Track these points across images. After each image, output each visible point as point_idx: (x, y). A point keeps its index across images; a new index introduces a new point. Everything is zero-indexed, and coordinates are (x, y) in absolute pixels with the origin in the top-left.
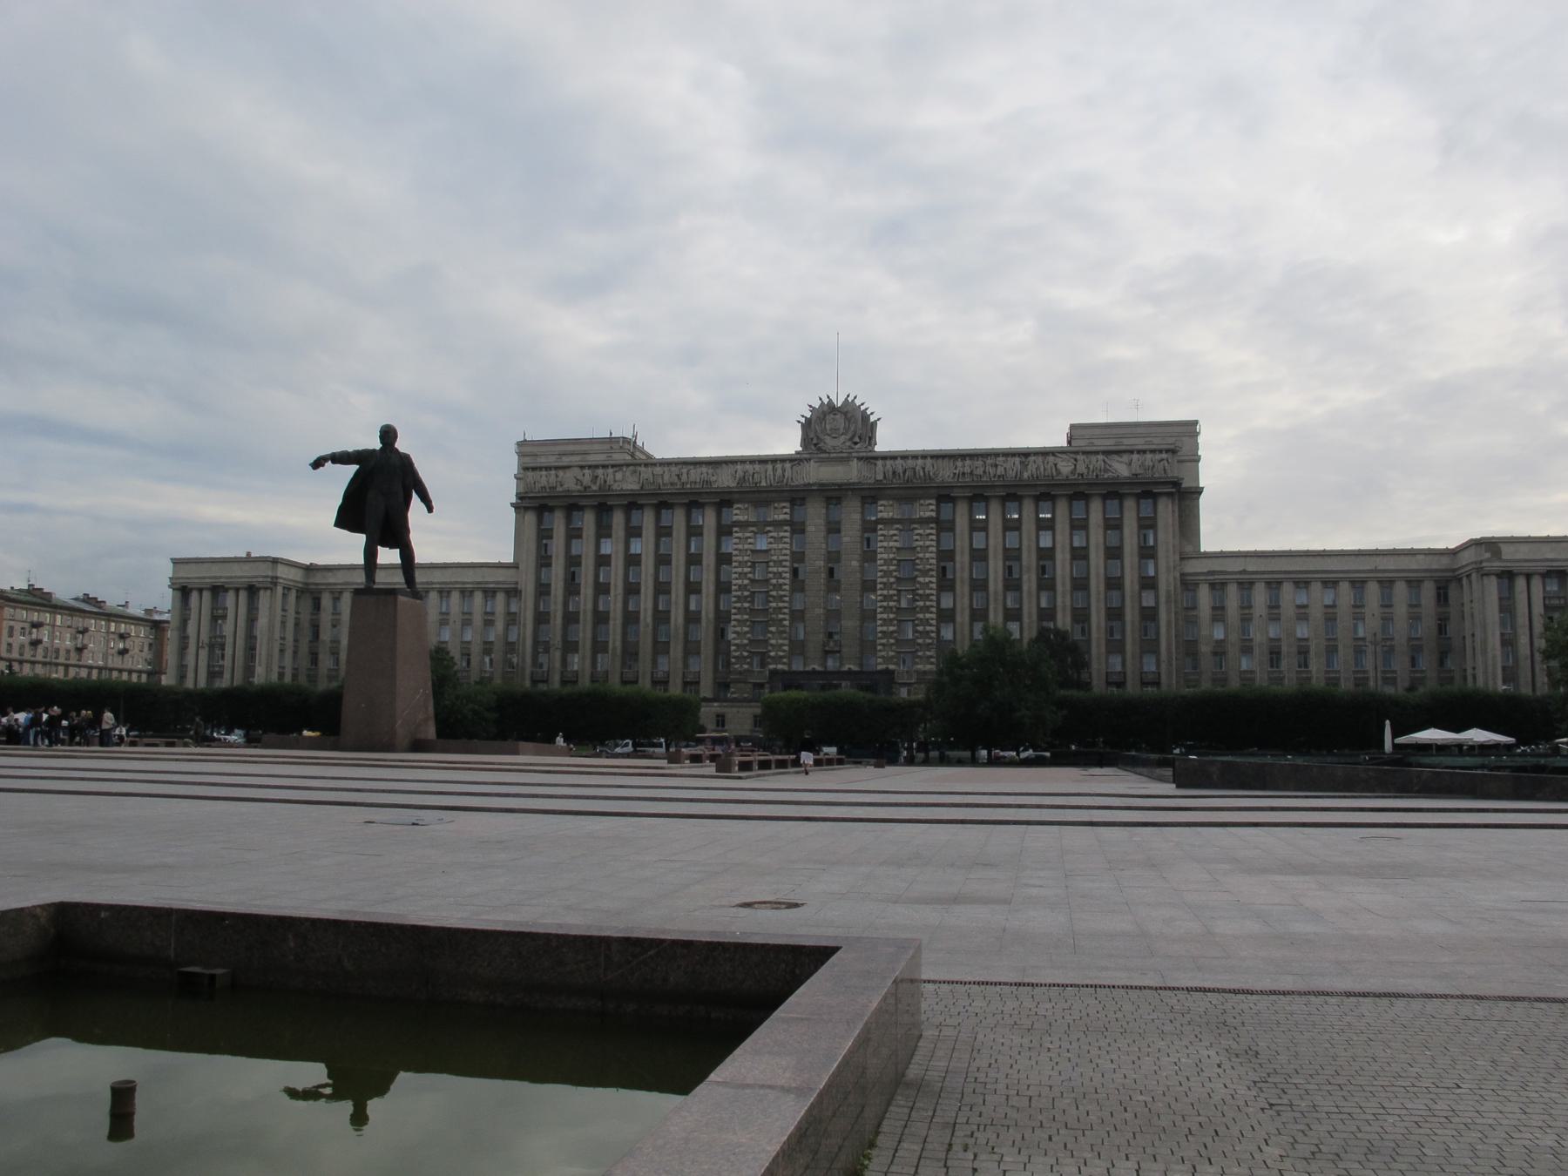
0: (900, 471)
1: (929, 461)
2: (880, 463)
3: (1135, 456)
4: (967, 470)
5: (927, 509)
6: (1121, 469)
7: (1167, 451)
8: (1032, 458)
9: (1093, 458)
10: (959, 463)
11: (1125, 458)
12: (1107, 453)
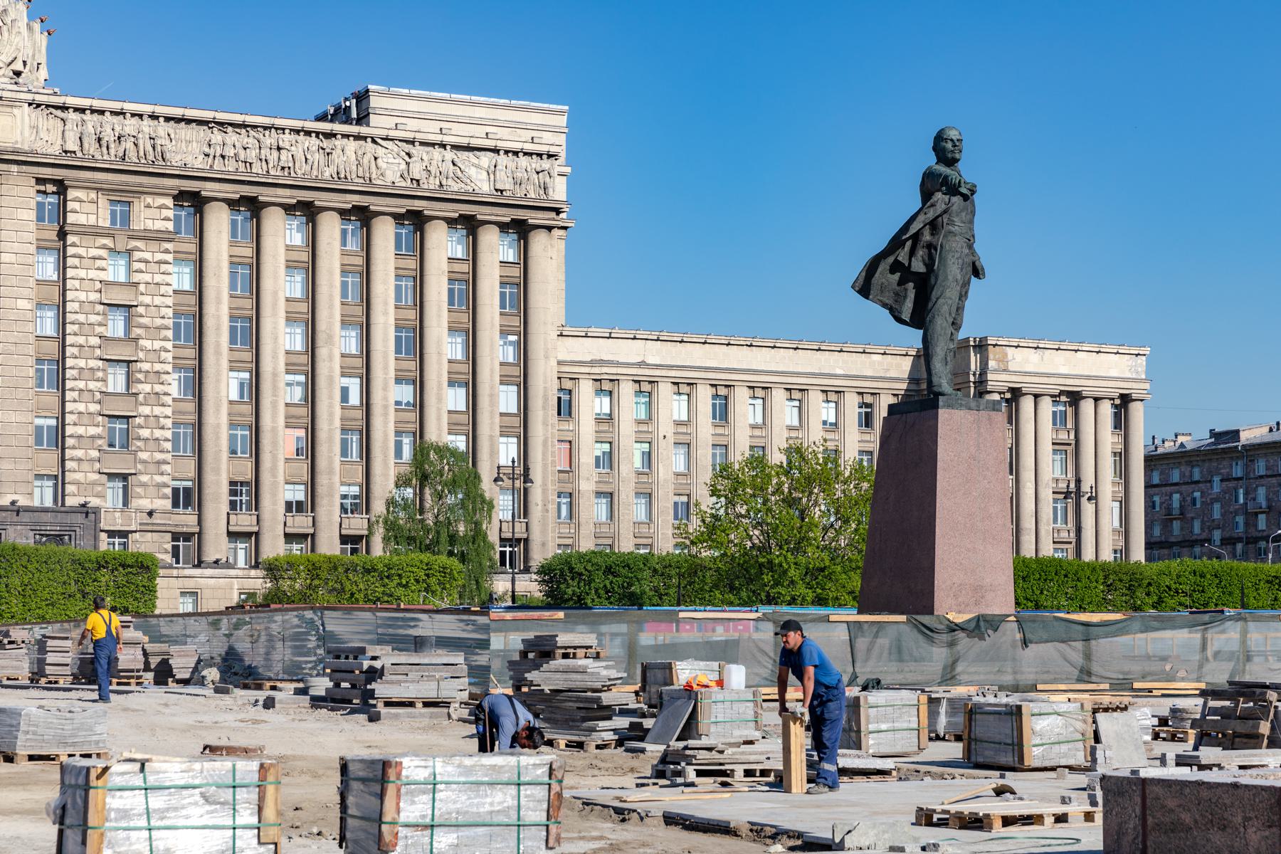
0: (108, 136)
1: (163, 128)
2: (72, 116)
3: (502, 159)
4: (230, 152)
5: (155, 213)
6: (478, 177)
7: (550, 156)
8: (339, 142)
9: (437, 152)
10: (217, 137)
11: (486, 159)
12: (456, 147)
